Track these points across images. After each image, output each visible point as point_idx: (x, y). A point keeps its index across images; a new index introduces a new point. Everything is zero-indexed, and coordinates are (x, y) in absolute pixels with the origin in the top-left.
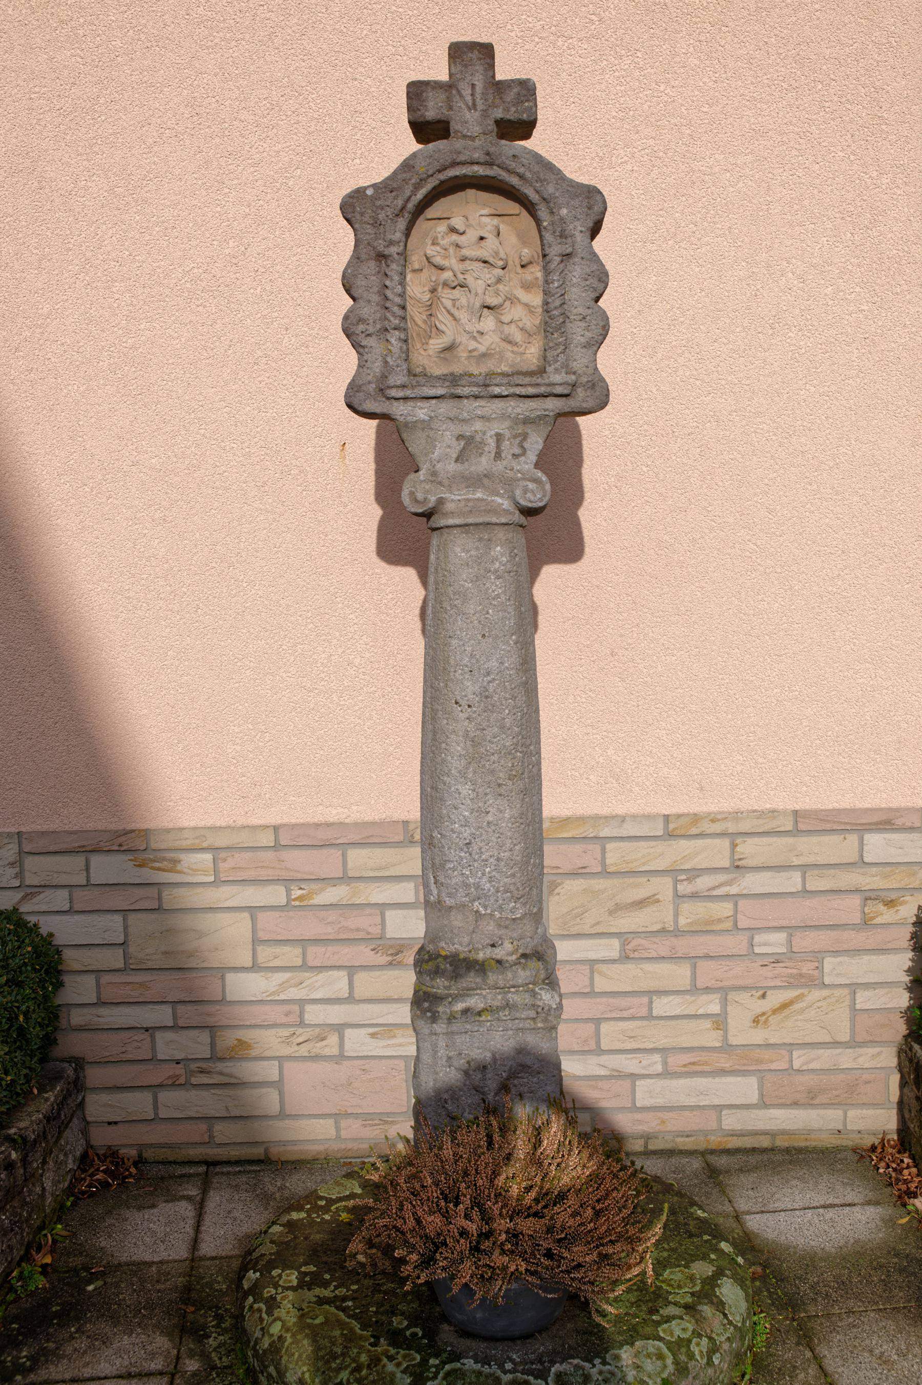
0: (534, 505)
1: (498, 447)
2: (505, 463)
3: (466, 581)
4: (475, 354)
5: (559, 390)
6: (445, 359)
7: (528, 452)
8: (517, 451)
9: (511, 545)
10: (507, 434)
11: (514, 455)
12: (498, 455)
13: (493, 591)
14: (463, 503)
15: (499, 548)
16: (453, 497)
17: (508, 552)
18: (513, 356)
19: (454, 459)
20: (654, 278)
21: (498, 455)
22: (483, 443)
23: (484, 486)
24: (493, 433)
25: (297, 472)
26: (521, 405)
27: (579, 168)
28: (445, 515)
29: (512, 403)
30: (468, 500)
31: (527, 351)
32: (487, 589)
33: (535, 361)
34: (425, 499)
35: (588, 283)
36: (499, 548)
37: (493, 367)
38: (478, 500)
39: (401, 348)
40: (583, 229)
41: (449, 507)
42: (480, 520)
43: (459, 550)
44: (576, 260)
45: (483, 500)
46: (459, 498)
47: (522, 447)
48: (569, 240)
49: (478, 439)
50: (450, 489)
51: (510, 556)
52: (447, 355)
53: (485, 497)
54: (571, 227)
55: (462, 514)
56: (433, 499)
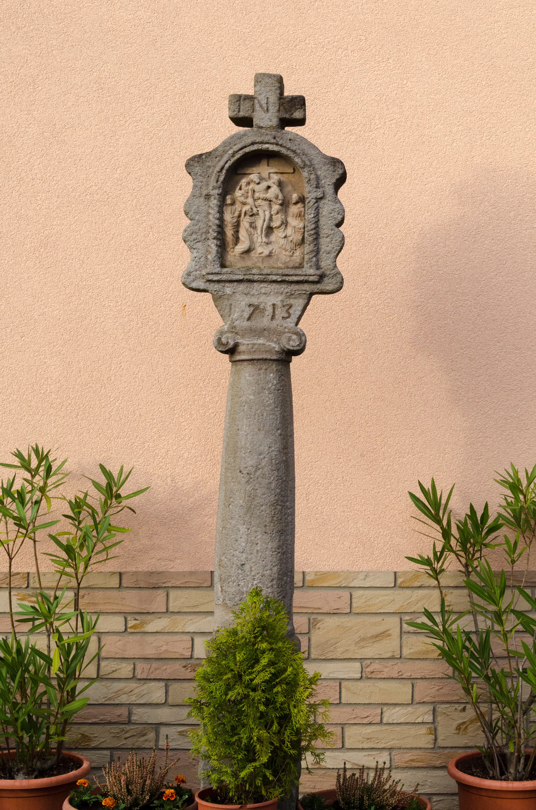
0: (295, 348)
1: (274, 312)
2: (278, 322)
3: (250, 395)
4: (262, 255)
5: (311, 278)
6: (244, 258)
7: (292, 316)
8: (286, 315)
9: (279, 373)
10: (279, 304)
11: (283, 317)
12: (273, 318)
13: (267, 402)
14: (250, 346)
15: (272, 375)
16: (244, 342)
17: (278, 378)
18: (285, 257)
19: (246, 319)
20: (397, 203)
21: (273, 318)
22: (264, 309)
23: (264, 336)
24: (271, 303)
25: (152, 323)
26: (289, 287)
27: (350, 130)
28: (240, 353)
29: (284, 286)
30: (254, 344)
31: (294, 255)
32: (263, 400)
33: (298, 261)
34: (228, 342)
35: (332, 215)
36: (272, 375)
37: (272, 264)
38: (260, 344)
39: (217, 251)
40: (330, 184)
41: (241, 348)
42: (261, 357)
43: (247, 375)
44: (326, 201)
45: (263, 344)
46: (249, 342)
47: (289, 313)
48: (321, 189)
49: (261, 307)
50: (243, 337)
51: (279, 380)
52: (245, 256)
53: (265, 343)
54: (323, 181)
55: (250, 353)
56: (231, 343)
